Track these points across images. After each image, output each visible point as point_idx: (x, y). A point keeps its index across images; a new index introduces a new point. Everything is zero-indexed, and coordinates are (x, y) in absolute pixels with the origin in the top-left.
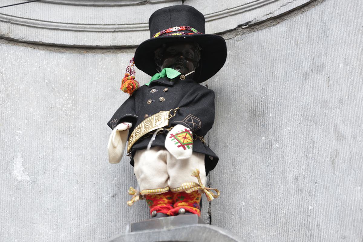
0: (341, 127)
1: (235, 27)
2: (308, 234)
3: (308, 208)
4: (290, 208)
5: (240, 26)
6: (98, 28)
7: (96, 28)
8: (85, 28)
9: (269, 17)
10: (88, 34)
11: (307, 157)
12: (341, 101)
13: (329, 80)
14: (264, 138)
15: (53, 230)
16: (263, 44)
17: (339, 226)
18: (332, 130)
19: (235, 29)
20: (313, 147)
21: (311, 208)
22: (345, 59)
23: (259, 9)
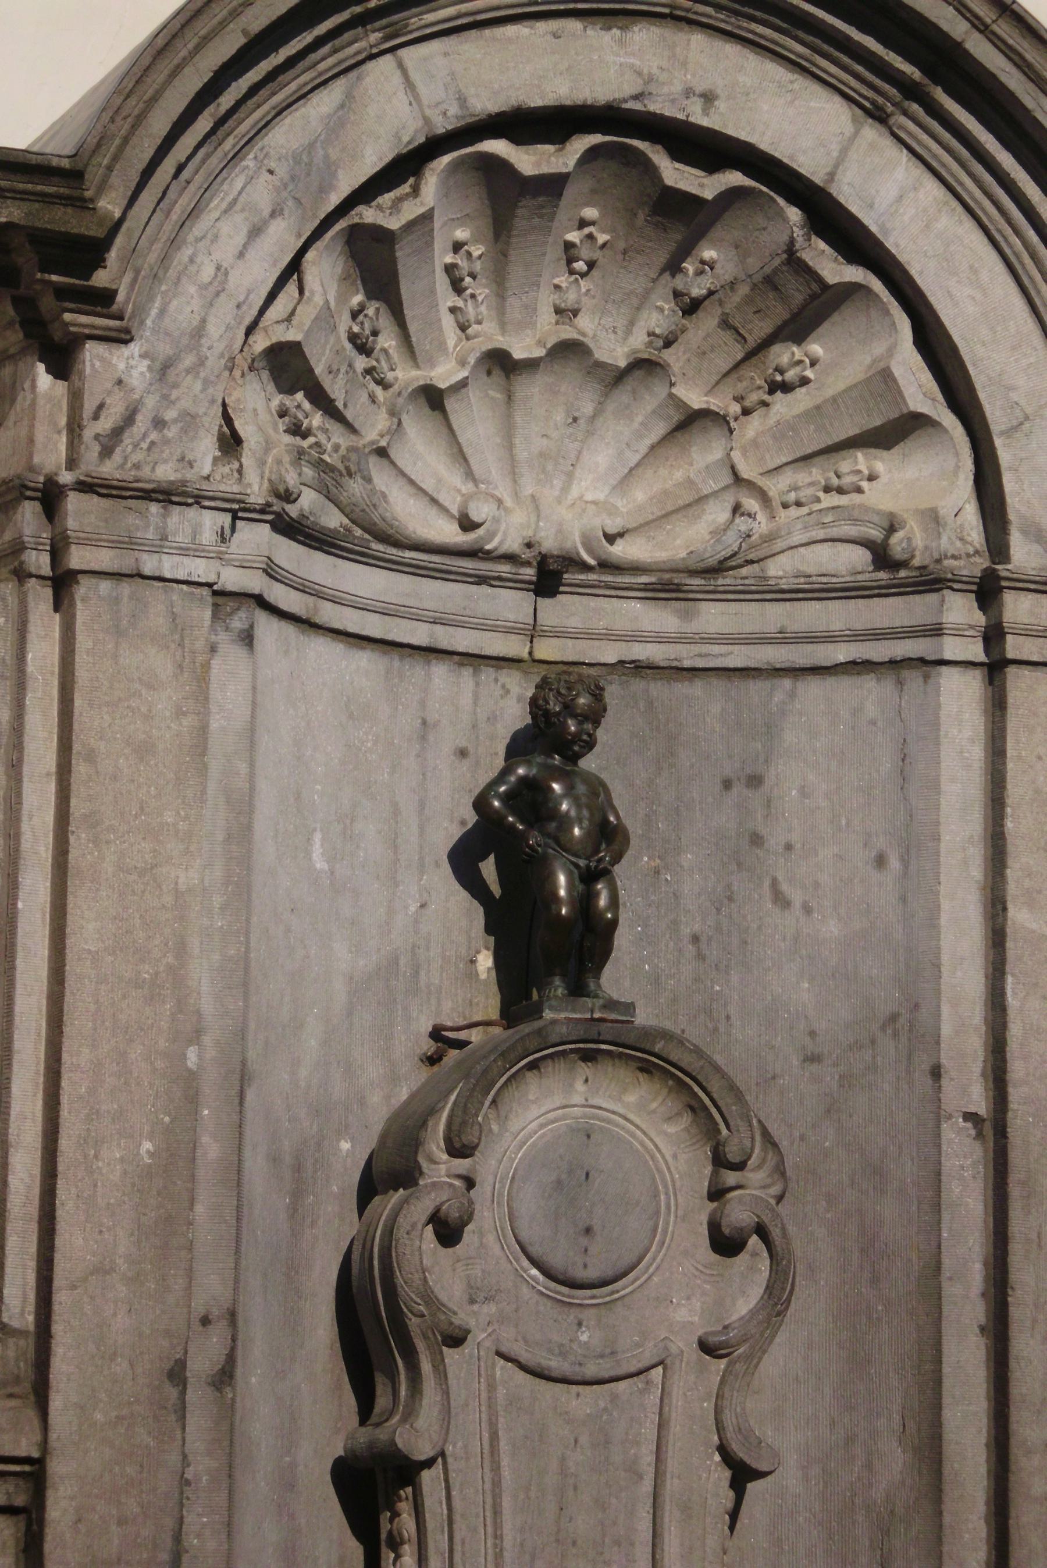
0: (784, 887)
1: (613, 661)
2: (710, 1025)
3: (713, 987)
4: (683, 979)
5: (621, 662)
6: (413, 614)
7: (411, 613)
8: (398, 611)
9: (675, 664)
10: (399, 620)
11: (718, 910)
12: (789, 847)
13: (769, 806)
14: (646, 859)
15: (351, 953)
16: (656, 704)
17: (763, 1028)
18: (767, 883)
19: (612, 665)
20: (730, 899)
21: (718, 988)
22: (804, 787)
23: (658, 645)
